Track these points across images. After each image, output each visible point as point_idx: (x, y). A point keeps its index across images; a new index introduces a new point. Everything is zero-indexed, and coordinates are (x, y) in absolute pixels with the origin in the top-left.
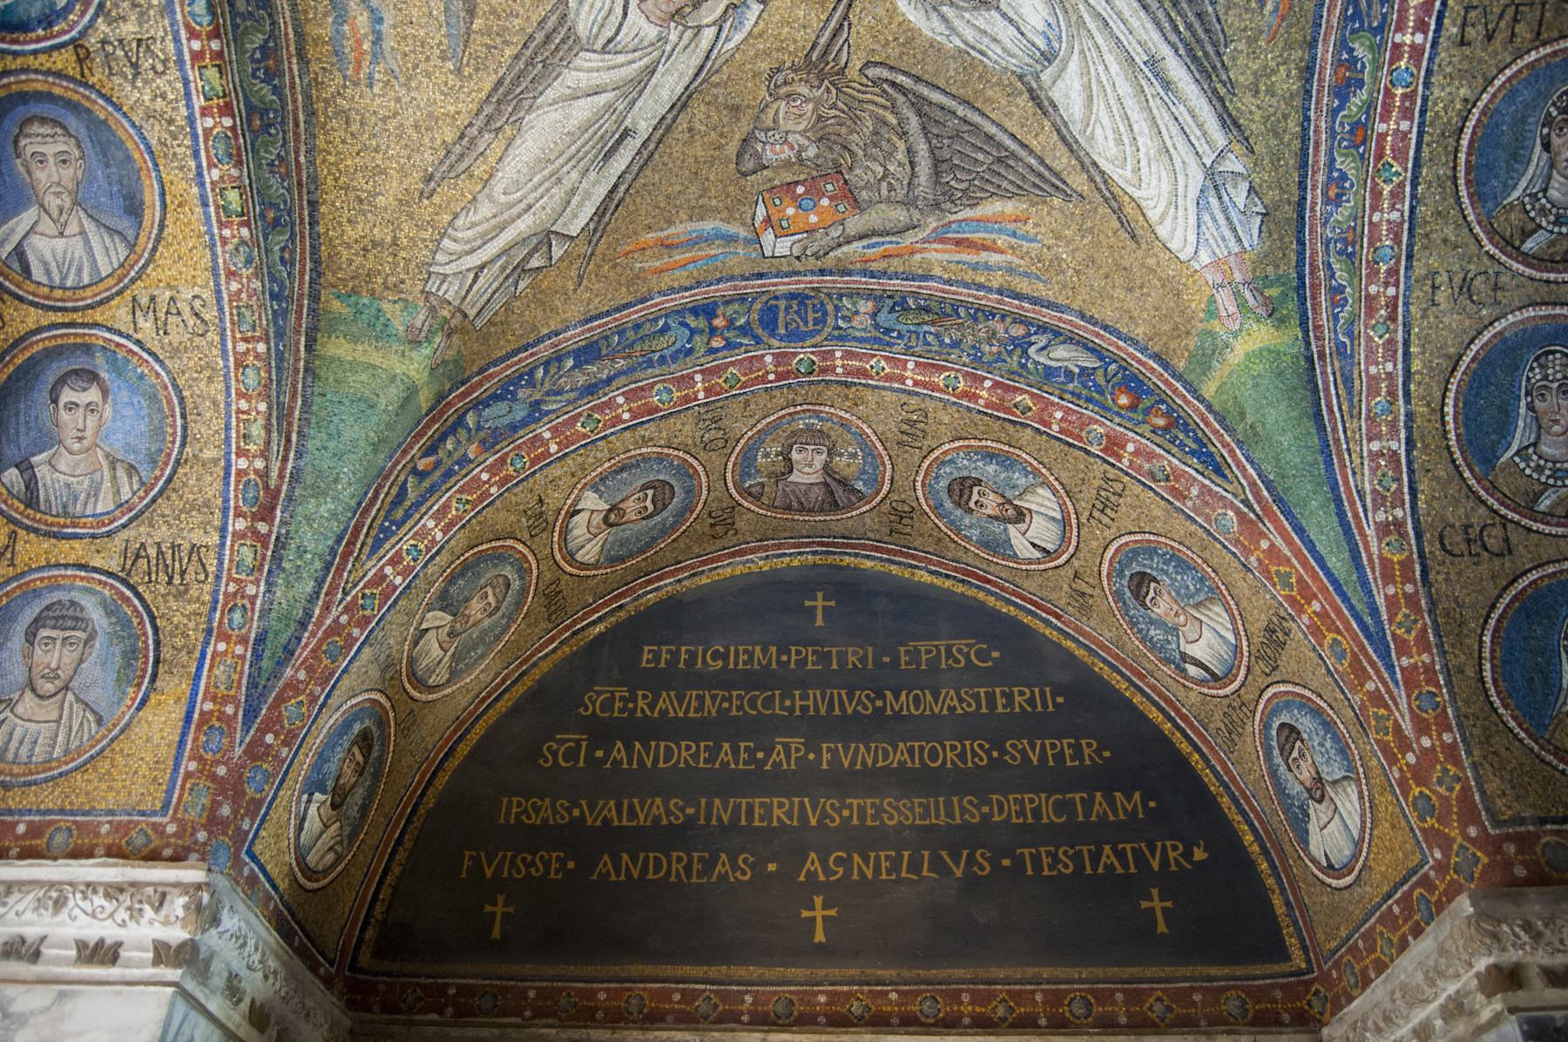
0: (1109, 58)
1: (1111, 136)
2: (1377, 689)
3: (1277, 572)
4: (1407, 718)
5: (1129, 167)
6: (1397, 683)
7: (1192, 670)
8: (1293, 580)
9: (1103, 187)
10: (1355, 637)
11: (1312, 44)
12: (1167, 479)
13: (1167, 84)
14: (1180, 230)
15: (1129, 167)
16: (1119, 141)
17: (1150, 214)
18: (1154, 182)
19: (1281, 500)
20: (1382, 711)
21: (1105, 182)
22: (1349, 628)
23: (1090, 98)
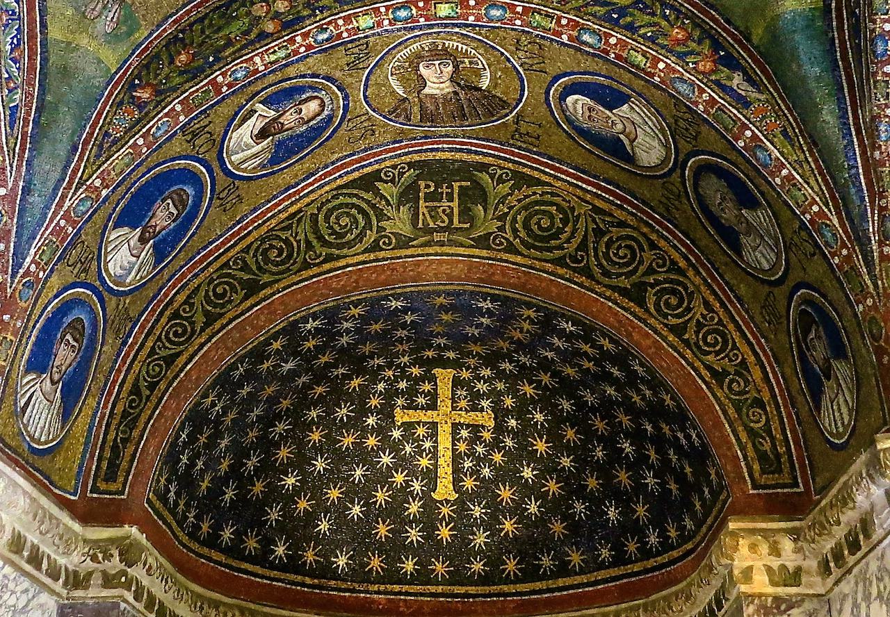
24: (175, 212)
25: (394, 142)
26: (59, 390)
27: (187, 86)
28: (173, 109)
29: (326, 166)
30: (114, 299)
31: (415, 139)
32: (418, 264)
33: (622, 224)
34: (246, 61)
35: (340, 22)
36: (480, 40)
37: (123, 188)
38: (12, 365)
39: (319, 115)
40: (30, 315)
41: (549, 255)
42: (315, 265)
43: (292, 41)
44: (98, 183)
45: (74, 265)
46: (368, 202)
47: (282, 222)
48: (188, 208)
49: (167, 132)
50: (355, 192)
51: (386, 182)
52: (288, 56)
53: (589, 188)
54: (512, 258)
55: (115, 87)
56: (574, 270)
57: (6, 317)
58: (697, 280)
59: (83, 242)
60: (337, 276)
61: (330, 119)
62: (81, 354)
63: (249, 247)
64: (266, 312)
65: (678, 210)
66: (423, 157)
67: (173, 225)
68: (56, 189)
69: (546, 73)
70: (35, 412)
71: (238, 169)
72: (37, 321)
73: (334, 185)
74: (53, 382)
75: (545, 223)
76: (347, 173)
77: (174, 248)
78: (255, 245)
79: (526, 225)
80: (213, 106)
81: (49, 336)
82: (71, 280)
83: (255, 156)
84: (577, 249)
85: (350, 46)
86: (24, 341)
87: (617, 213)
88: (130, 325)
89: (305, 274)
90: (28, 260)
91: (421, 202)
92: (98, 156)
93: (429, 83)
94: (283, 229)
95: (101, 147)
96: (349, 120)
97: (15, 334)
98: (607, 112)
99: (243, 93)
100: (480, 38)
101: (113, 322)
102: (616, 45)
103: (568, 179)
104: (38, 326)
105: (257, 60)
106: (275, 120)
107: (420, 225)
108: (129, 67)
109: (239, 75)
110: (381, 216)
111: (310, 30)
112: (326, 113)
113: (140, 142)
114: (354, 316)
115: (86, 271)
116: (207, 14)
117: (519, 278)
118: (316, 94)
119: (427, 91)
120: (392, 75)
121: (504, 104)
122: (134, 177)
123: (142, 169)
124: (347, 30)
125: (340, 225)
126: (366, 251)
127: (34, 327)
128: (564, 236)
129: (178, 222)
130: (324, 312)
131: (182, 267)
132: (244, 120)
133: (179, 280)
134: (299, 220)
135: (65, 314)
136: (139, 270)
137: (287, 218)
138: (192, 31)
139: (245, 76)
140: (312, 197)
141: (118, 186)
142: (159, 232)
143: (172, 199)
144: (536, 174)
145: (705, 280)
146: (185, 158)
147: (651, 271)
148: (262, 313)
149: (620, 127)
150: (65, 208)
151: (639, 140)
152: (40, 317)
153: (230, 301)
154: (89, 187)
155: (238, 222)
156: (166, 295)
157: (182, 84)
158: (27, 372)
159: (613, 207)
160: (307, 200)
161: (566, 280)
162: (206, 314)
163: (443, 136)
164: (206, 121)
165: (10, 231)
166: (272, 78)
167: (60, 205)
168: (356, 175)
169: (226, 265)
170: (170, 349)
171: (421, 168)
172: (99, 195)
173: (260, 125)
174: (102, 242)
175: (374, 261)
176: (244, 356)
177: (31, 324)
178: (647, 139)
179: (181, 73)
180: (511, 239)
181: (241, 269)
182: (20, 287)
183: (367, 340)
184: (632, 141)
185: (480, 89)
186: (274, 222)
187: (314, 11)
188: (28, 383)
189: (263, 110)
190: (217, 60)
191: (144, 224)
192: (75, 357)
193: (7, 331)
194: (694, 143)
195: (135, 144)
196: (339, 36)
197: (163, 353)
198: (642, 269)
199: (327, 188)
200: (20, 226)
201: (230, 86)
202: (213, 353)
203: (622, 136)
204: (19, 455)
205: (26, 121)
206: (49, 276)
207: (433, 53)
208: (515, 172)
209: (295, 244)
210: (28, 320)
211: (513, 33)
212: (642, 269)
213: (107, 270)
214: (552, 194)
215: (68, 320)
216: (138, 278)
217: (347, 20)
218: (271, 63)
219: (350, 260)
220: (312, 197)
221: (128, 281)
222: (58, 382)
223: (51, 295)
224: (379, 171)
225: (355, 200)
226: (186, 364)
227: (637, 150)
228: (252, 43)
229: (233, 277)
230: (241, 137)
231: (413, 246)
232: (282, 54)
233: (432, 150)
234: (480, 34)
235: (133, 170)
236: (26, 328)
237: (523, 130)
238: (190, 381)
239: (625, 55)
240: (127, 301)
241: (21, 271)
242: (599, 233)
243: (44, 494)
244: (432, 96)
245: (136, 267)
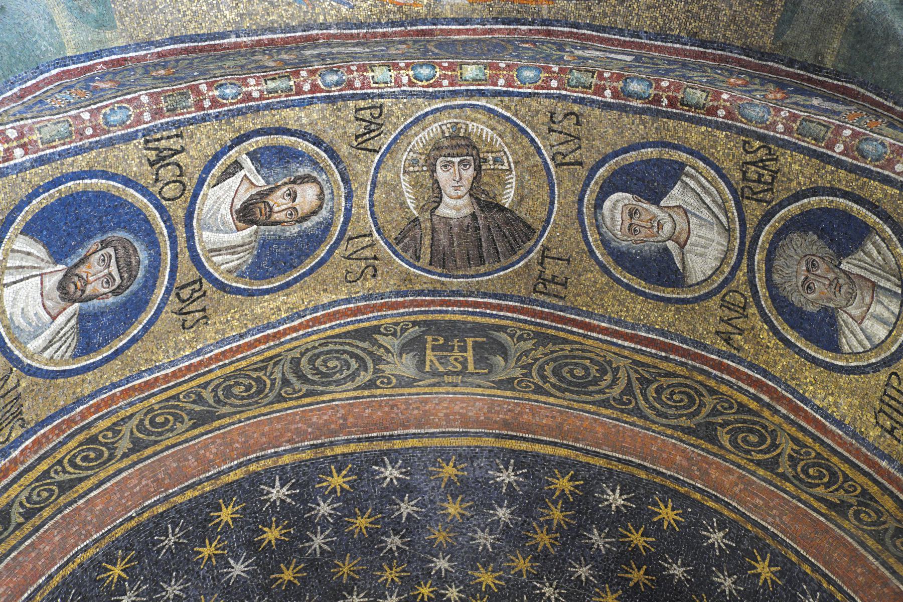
25: (398, 294)
29: (316, 309)
31: (420, 293)
32: (426, 401)
33: (669, 375)
36: (508, 119)
37: (47, 172)
39: (315, 213)
41: (590, 398)
42: (291, 399)
46: (364, 350)
47: (256, 363)
48: (134, 287)
50: (348, 341)
51: (387, 335)
53: (626, 344)
54: (544, 398)
56: (622, 411)
58: (776, 419)
60: (319, 409)
61: (327, 226)
63: (208, 383)
64: (218, 441)
65: (741, 332)
66: (430, 317)
67: (111, 300)
69: (581, 164)
73: (322, 335)
75: (579, 372)
76: (340, 325)
78: (217, 382)
79: (556, 372)
83: (232, 249)
84: (622, 393)
85: (362, 104)
87: (664, 365)
89: (277, 406)
91: (428, 352)
93: (446, 199)
94: (256, 370)
96: (351, 239)
98: (654, 209)
100: (509, 114)
102: (669, 87)
103: (600, 336)
107: (427, 368)
109: (228, 91)
110: (378, 360)
111: (317, 70)
112: (324, 213)
114: (334, 490)
117: (554, 417)
118: (315, 174)
119: (443, 211)
120: (405, 172)
121: (528, 231)
125: (327, 367)
126: (354, 389)
128: (603, 384)
130: (297, 466)
131: (114, 386)
132: (227, 174)
133: (107, 403)
134: (275, 364)
136: (51, 343)
137: (262, 361)
140: (295, 344)
144: (562, 334)
145: (786, 418)
146: (144, 191)
147: (714, 412)
148: (213, 443)
149: (667, 227)
151: (693, 238)
153: (172, 430)
155: (198, 353)
156: (83, 416)
159: (657, 361)
160: (288, 346)
161: (613, 419)
162: (135, 442)
163: (454, 293)
168: (351, 328)
169: (176, 397)
170: (70, 473)
171: (428, 325)
175: (369, 397)
176: (178, 509)
178: (704, 232)
180: (540, 383)
181: (194, 402)
183: (347, 550)
184: (682, 246)
185: (502, 209)
186: (244, 363)
189: (250, 171)
194: (768, 196)
197: (61, 477)
198: (704, 411)
199: (314, 337)
202: (135, 481)
203: (670, 245)
207: (454, 142)
208: (537, 335)
209: (268, 382)
211: (547, 102)
212: (704, 411)
214: (583, 351)
219: (337, 396)
220: (295, 344)
224: (379, 326)
225: (347, 348)
226: (91, 490)
227: (689, 257)
229: (181, 409)
231: (419, 386)
233: (440, 312)
234: (508, 108)
237: (548, 274)
238: (92, 511)
239: (680, 96)
242: (645, 382)
244: (446, 220)
245: (47, 334)
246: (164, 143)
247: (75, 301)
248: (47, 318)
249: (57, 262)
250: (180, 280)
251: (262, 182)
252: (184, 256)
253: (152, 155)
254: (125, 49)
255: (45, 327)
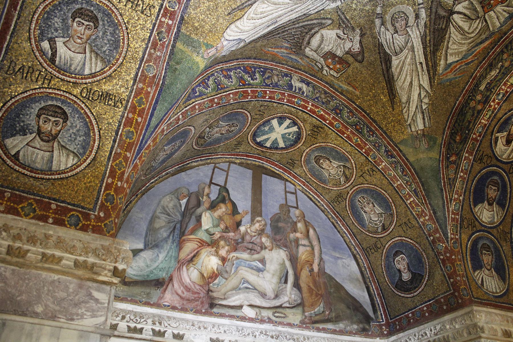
0: (283, 11)
1: (264, 10)
2: (129, 158)
3: (141, 98)
4: (128, 174)
5: (254, 16)
6: (133, 163)
7: (46, 45)
8: (143, 106)
9: (247, 4)
10: (138, 140)
11: (255, 59)
12: (160, 40)
13: (268, 26)
14: (233, 34)
15: (254, 16)
16: (262, 13)
17: (238, 22)
18: (248, 25)
19: (162, 90)
20: (124, 164)
21: (249, 5)
22: (140, 136)
23: (276, 4)
24: (496, 188)
26: (493, 272)
27: (465, 146)
28: (465, 157)
30: (495, 230)
34: (479, 124)
35: (503, 87)
38: (466, 271)
40: (462, 252)
43: (490, 106)
44: (456, 196)
45: (468, 227)
48: (500, 184)
49: (469, 165)
52: (493, 112)
55: (442, 162)
57: (453, 257)
59: (466, 218)
62: (494, 255)
67: (499, 193)
68: (444, 207)
70: (488, 283)
71: (509, 159)
72: (466, 253)
74: (488, 270)
77: (506, 200)
80: (479, 146)
81: (475, 255)
82: (470, 233)
86: (465, 261)
88: (509, 235)
90: (449, 234)
92: (451, 188)
95: (450, 184)
97: (460, 261)
99: (487, 135)
101: (500, 238)
104: (468, 254)
105: (483, 121)
106: (509, 135)
108: (443, 153)
111: (494, 98)
113: (462, 174)
115: (475, 226)
116: (457, 119)
122: (469, 187)
123: (470, 182)
124: (508, 88)
127: (466, 255)
129: (500, 190)
132: (496, 143)
135: (477, 245)
136: (498, 215)
138: (455, 127)
139: (483, 129)
141: (465, 193)
142: (495, 198)
143: (491, 185)
146: (484, 169)
150: (451, 211)
152: (466, 251)
154: (455, 199)
157: (463, 147)
158: (474, 271)
164: (481, 152)
165: (437, 229)
166: (494, 123)
167: (448, 211)
172: (460, 200)
173: (504, 140)
174: (473, 214)
177: (464, 255)
179: (461, 143)
182: (452, 245)
187: (491, 91)
188: (477, 275)
190: (469, 131)
191: (486, 199)
192: (492, 257)
193: (456, 261)
195: (461, 176)
196: (507, 92)
200: (440, 225)
201: (480, 136)
204: (491, 301)
205: (421, 191)
206: (460, 236)
210: (462, 254)
213: (483, 222)
215: (480, 246)
216: (499, 218)
217: (505, 84)
218: (489, 118)
221: (495, 221)
222: (491, 269)
223: (466, 242)
228: (477, 116)
230: (500, 149)
232: (490, 113)
235: (466, 185)
236: (463, 257)
240: (501, 228)
241: (449, 239)
243: (508, 311)
245: (495, 214)
246: (479, 157)
247: (493, 203)
248: (492, 212)
249: (484, 202)
250: (507, 171)
251: (505, 133)
252: (503, 166)
253: (479, 161)
254: (443, 138)
255: (494, 214)
